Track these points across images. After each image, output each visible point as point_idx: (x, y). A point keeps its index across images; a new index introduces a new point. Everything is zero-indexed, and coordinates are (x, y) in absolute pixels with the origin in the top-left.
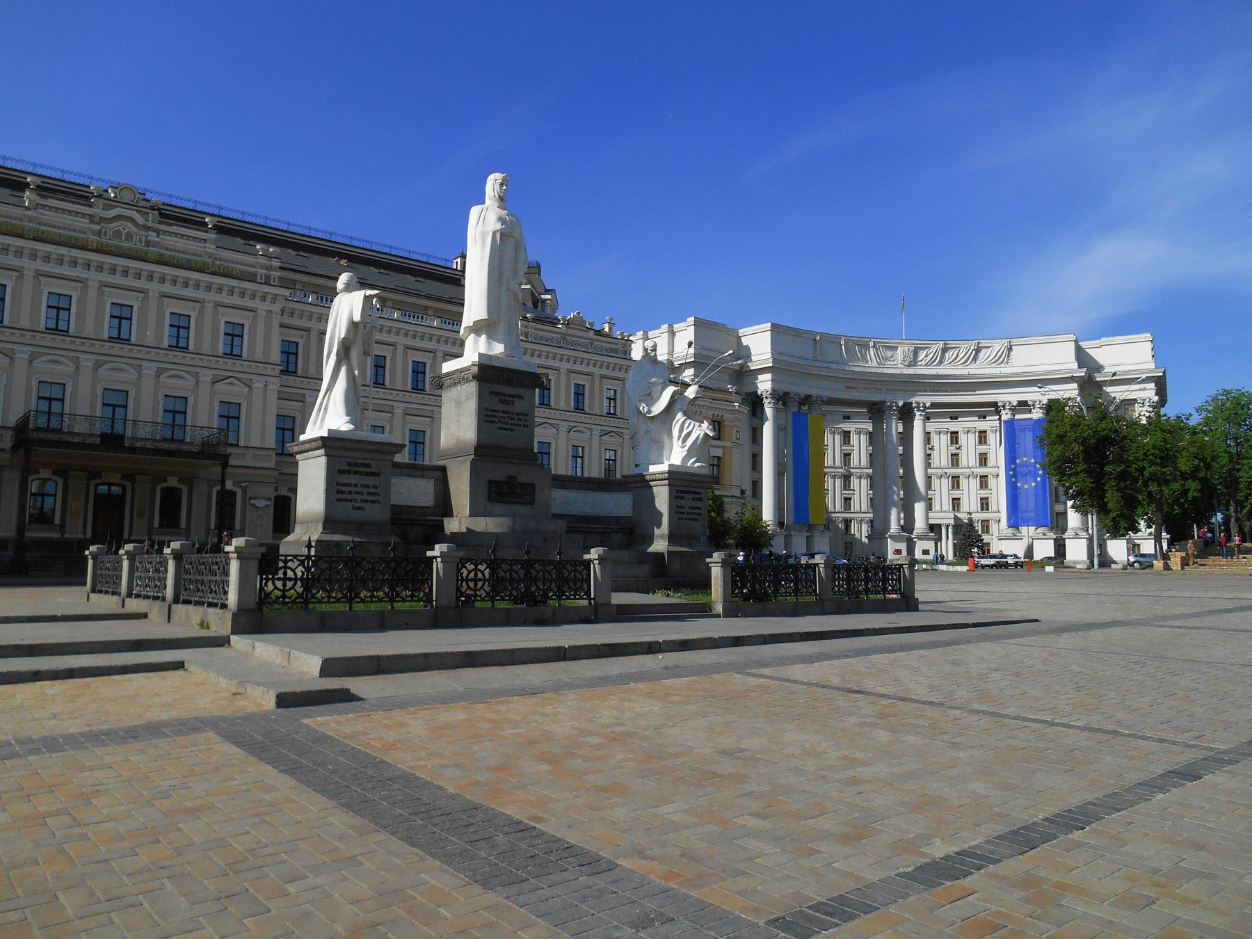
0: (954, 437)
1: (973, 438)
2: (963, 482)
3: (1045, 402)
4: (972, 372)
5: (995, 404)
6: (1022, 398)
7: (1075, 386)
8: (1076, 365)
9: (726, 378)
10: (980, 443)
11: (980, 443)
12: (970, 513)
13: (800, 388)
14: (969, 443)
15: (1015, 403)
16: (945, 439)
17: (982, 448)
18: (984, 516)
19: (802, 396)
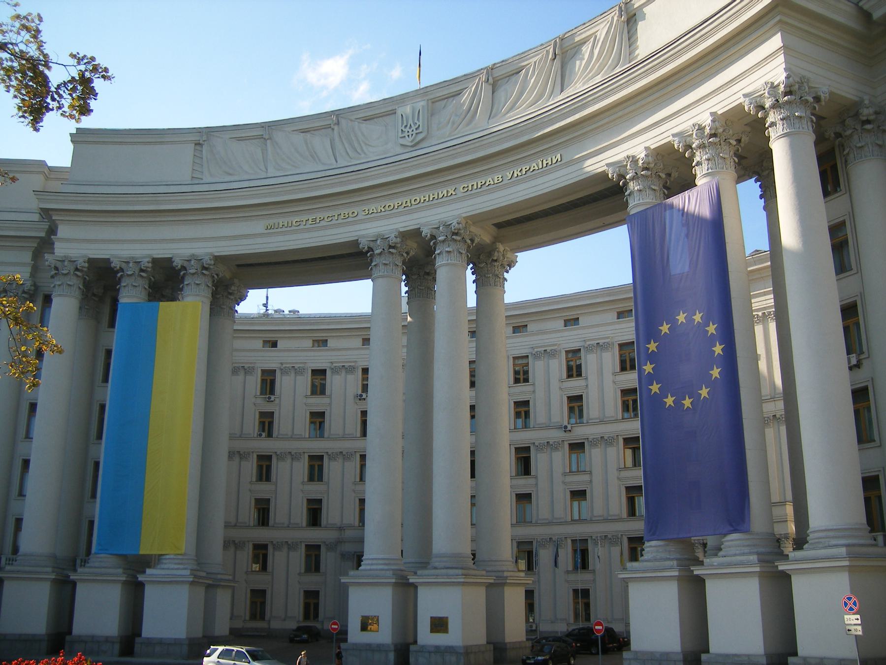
9: (27, 257)
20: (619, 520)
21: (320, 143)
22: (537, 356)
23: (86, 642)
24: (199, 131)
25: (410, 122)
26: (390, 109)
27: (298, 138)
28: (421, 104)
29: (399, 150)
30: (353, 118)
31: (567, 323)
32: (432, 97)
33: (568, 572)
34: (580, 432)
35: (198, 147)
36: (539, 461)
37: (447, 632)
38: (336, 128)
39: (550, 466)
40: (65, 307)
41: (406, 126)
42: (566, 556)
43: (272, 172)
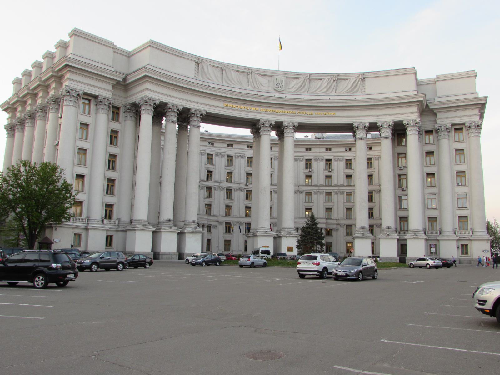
0: (329, 162)
1: (342, 164)
2: (335, 197)
3: (391, 123)
4: (332, 98)
5: (350, 128)
6: (373, 120)
7: (415, 109)
8: (416, 93)
9: (110, 87)
10: (347, 168)
11: (347, 168)
12: (337, 220)
13: (177, 100)
14: (339, 167)
15: (367, 125)
16: (322, 164)
17: (348, 172)
18: (349, 222)
19: (181, 108)
20: (242, 217)
21: (243, 78)
22: (237, 157)
23: (167, 255)
24: (198, 58)
25: (280, 83)
26: (271, 74)
27: (234, 74)
28: (284, 78)
29: (274, 91)
30: (256, 73)
31: (248, 147)
32: (287, 76)
33: (243, 234)
34: (250, 187)
35: (196, 64)
36: (235, 194)
37: (292, 251)
38: (250, 74)
39: (239, 197)
40: (147, 118)
41: (278, 84)
42: (243, 228)
43: (225, 84)
